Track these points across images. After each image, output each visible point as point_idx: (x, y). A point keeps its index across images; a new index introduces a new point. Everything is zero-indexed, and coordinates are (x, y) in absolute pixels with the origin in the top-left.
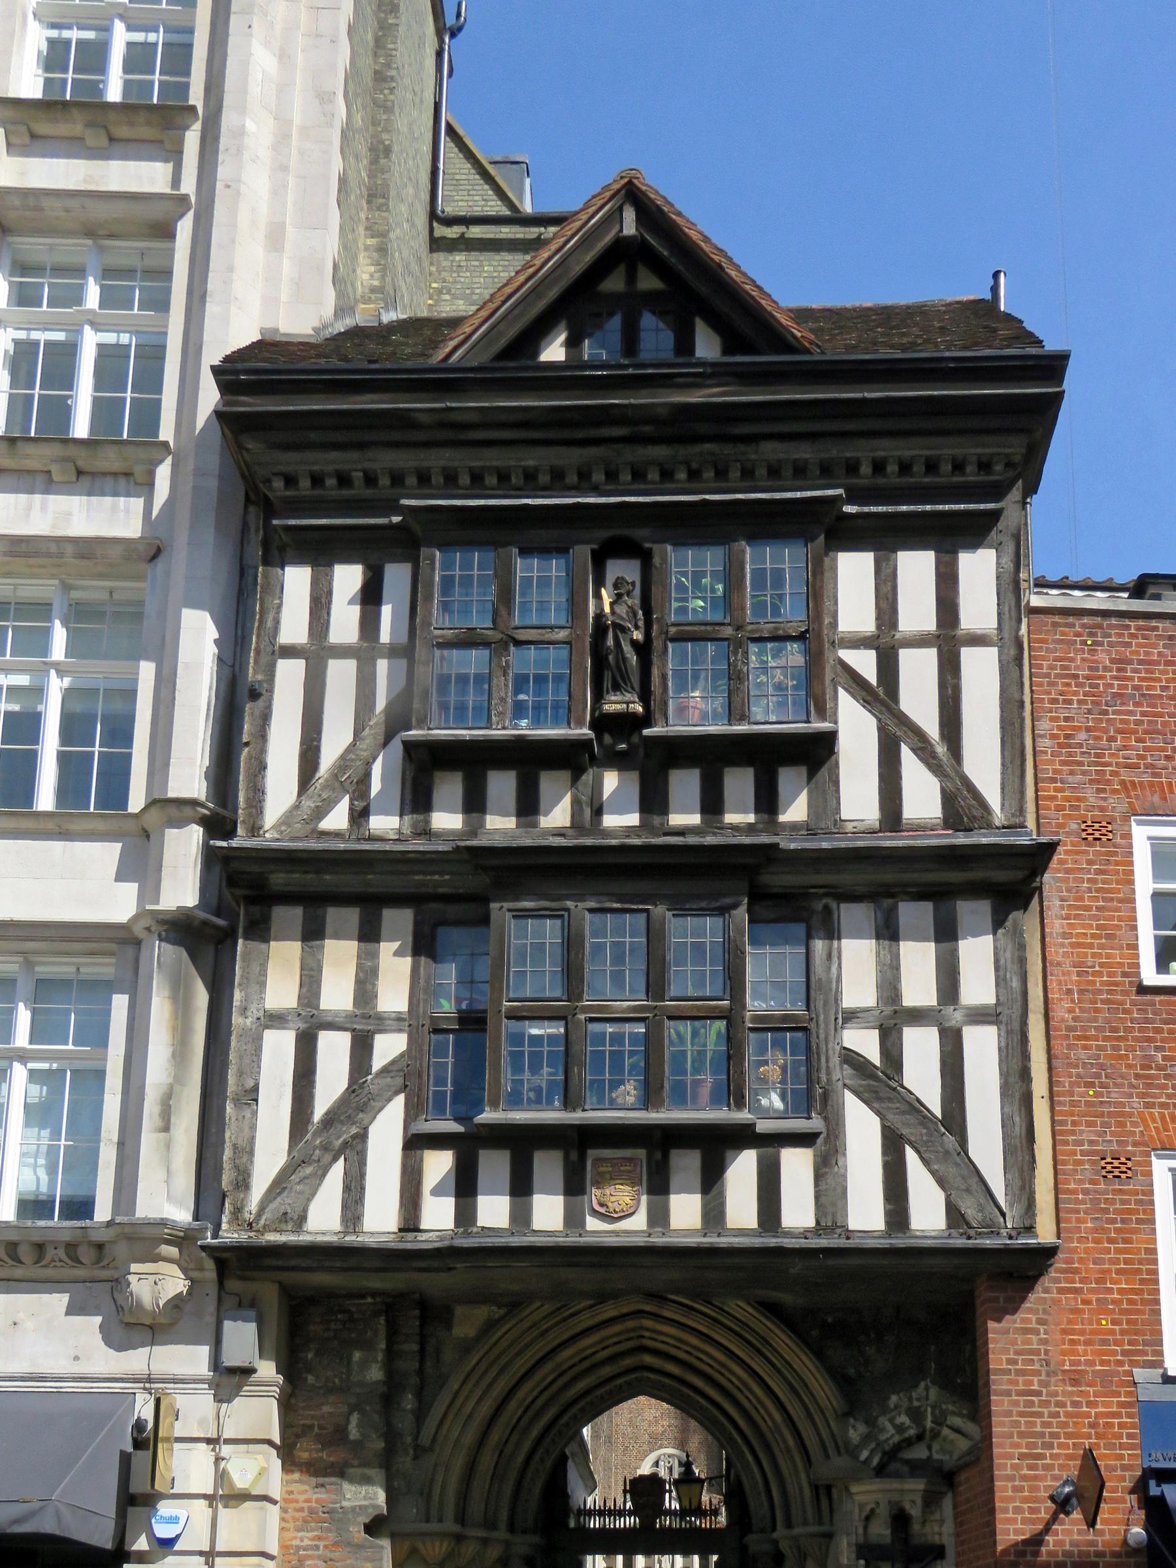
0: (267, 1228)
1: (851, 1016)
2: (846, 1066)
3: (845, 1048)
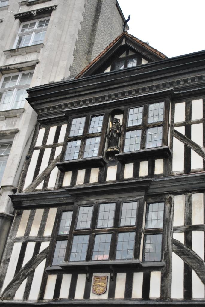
0: (4, 299)
1: (176, 229)
2: (173, 245)
3: (173, 239)
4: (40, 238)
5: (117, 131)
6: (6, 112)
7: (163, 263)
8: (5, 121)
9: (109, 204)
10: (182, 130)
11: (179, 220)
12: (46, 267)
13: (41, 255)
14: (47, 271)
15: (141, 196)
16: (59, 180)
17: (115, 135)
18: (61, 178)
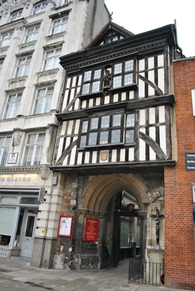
1: (141, 127)
4: (73, 135)
5: (109, 77)
6: (49, 71)
7: (135, 144)
8: (49, 76)
9: (107, 116)
10: (143, 75)
11: (142, 122)
12: (77, 149)
13: (74, 143)
14: (78, 151)
15: (123, 111)
16: (80, 105)
17: (107, 79)
18: (81, 104)
